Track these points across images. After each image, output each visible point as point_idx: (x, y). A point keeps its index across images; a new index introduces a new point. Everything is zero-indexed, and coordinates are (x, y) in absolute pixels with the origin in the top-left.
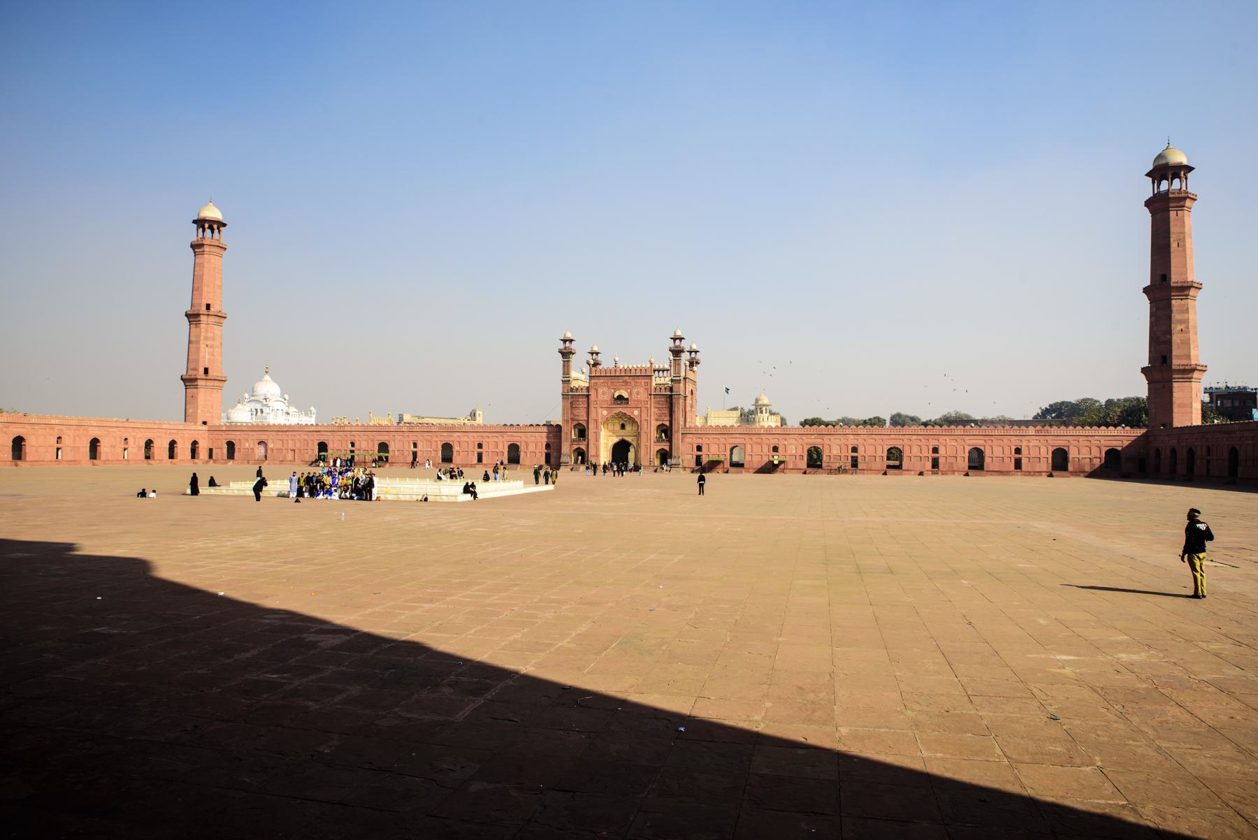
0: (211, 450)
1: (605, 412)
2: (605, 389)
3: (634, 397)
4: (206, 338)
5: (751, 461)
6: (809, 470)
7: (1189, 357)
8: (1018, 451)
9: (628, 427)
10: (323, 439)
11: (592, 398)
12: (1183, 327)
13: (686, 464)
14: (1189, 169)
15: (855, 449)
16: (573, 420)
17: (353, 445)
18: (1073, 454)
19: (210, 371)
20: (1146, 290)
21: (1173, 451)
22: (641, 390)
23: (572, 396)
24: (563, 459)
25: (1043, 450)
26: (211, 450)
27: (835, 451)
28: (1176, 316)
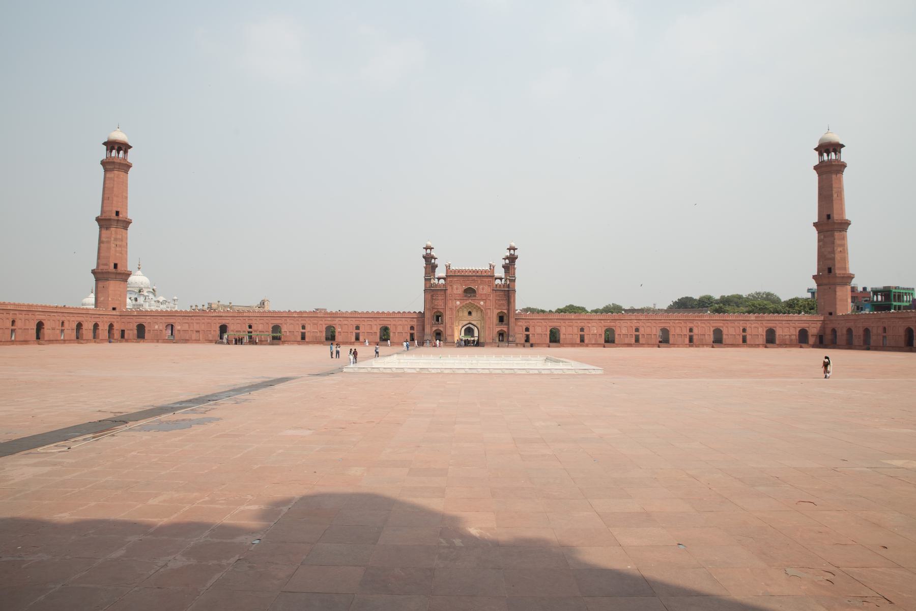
0: (123, 331)
1: (458, 303)
3: (480, 291)
4: (116, 239)
6: (606, 344)
8: (744, 330)
9: (474, 314)
10: (224, 322)
11: (449, 292)
13: (518, 341)
14: (842, 146)
15: (637, 330)
16: (433, 308)
17: (250, 327)
18: (779, 332)
19: (119, 266)
20: (815, 225)
21: (849, 331)
22: (486, 287)
23: (431, 291)
24: (426, 338)
26: (123, 331)
27: (624, 331)
28: (837, 242)
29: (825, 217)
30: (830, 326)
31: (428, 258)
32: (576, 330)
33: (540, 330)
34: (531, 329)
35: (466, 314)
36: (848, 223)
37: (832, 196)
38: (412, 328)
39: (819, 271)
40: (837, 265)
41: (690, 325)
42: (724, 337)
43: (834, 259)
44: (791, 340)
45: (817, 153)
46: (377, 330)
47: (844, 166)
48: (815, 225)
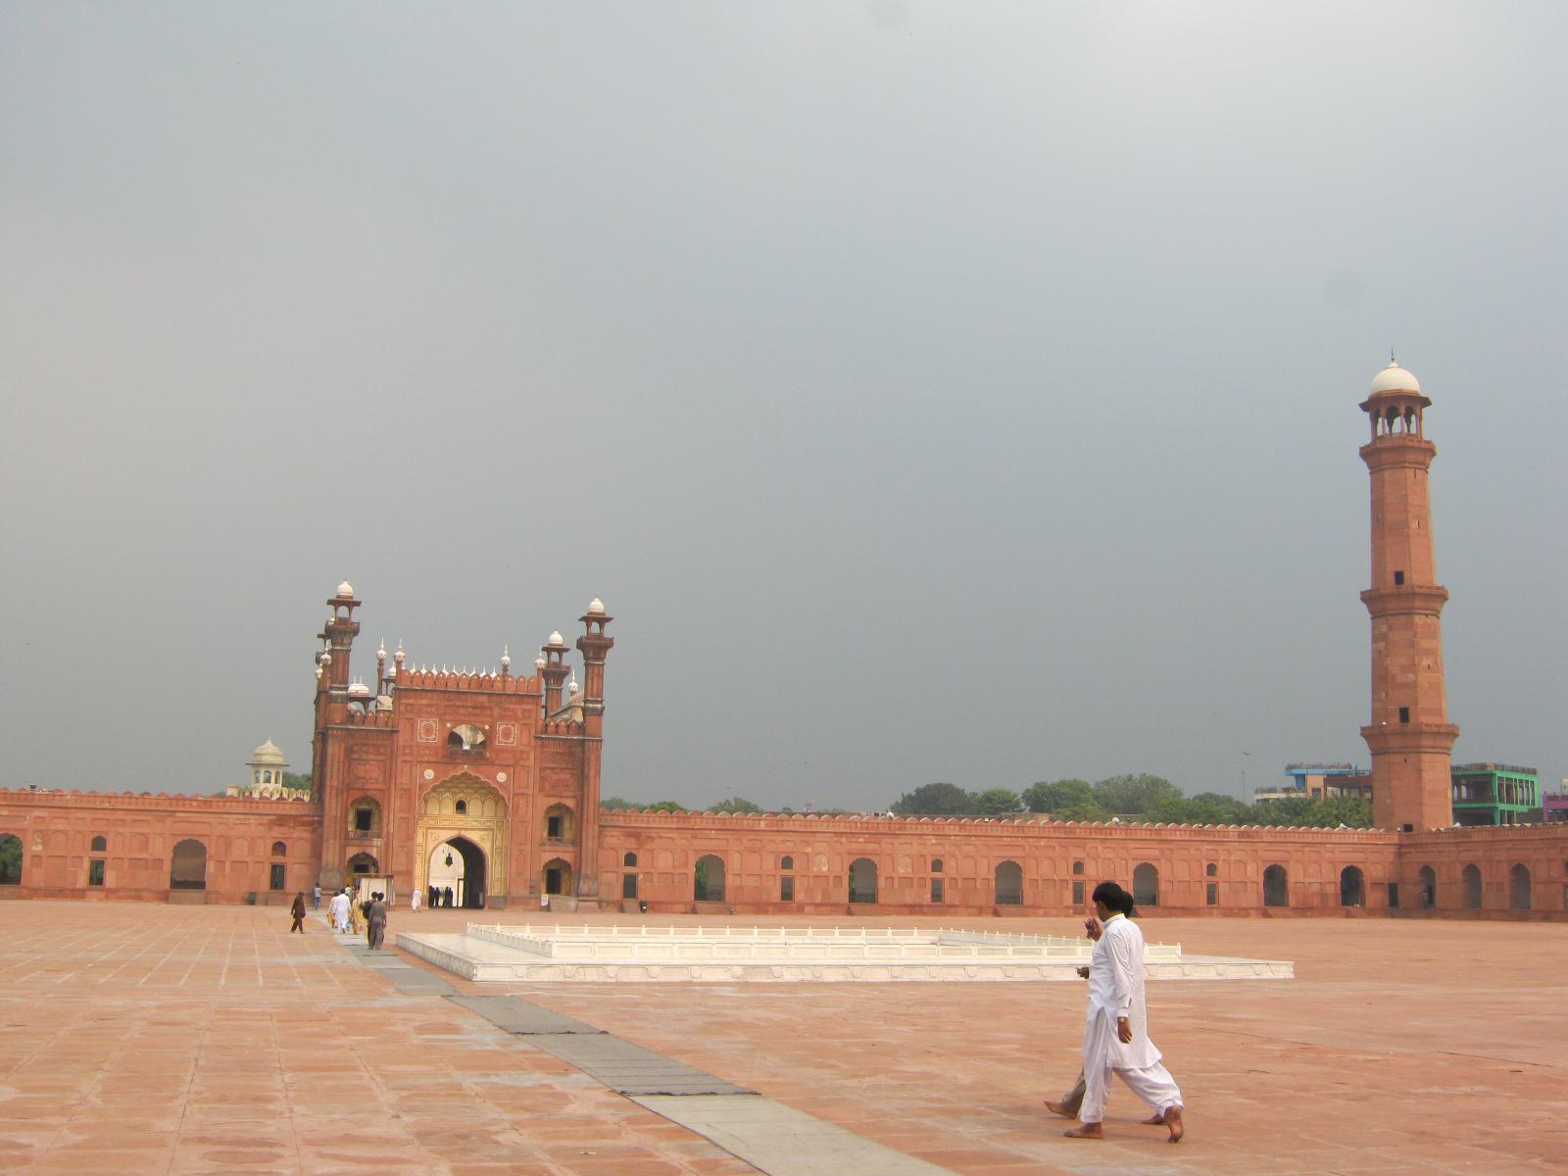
1: (429, 774)
2: (434, 723)
3: (499, 741)
5: (740, 888)
7: (1439, 712)
8: (1212, 869)
9: (474, 807)
11: (402, 739)
13: (604, 894)
14: (1426, 402)
15: (937, 865)
16: (348, 788)
18: (1295, 876)
20: (1367, 598)
22: (515, 730)
25: (1251, 868)
29: (1391, 579)
30: (1417, 859)
31: (339, 633)
32: (770, 863)
33: (668, 861)
34: (641, 859)
35: (449, 809)
36: (1441, 596)
37: (1406, 524)
38: (279, 847)
39: (1375, 715)
40: (1423, 704)
41: (1076, 854)
42: (1163, 886)
43: (1414, 686)
44: (1323, 895)
45: (1367, 415)
46: (162, 849)
47: (1430, 451)
48: (1367, 598)
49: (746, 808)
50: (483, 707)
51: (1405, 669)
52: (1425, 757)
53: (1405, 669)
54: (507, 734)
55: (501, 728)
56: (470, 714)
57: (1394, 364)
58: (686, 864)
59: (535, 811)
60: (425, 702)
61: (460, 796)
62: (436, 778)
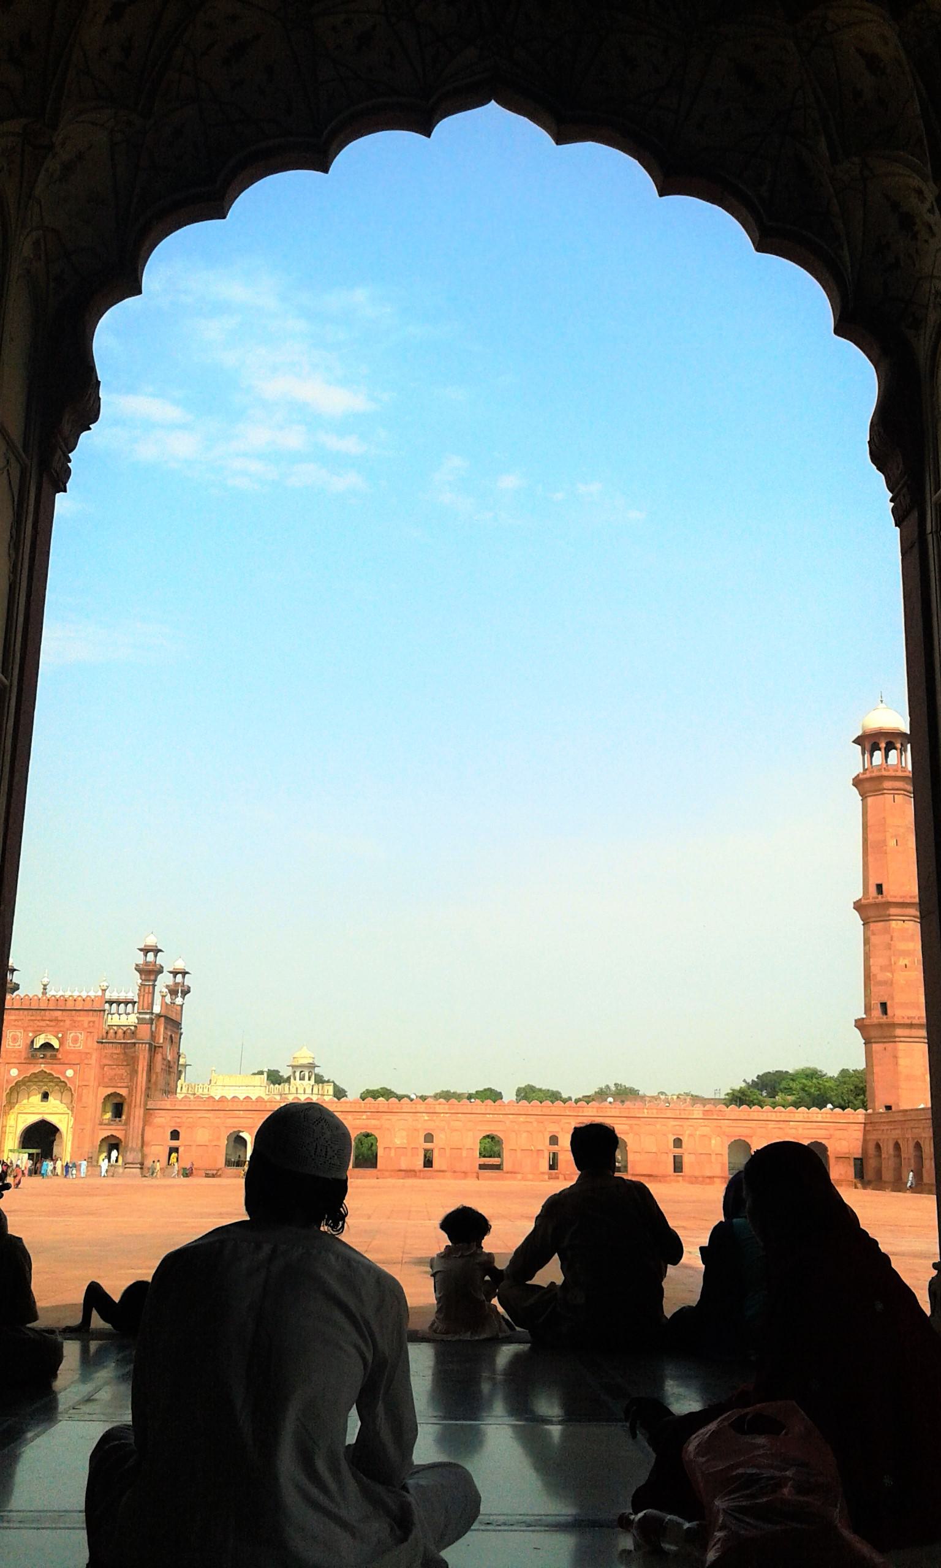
1: (14, 1072)
2: (19, 1034)
3: (69, 1045)
8: (678, 1143)
12: (906, 962)
15: (429, 1138)
22: (81, 1037)
29: (873, 890)
30: (873, 1137)
35: (37, 1098)
37: (884, 842)
43: (889, 983)
49: (386, 1093)
50: (56, 1020)
51: (883, 969)
52: (901, 1046)
53: (883, 969)
54: (75, 1040)
55: (71, 1036)
56: (48, 1025)
57: (883, 705)
58: (218, 1139)
59: (95, 1097)
60: (13, 1018)
61: (45, 1088)
62: (19, 1075)
